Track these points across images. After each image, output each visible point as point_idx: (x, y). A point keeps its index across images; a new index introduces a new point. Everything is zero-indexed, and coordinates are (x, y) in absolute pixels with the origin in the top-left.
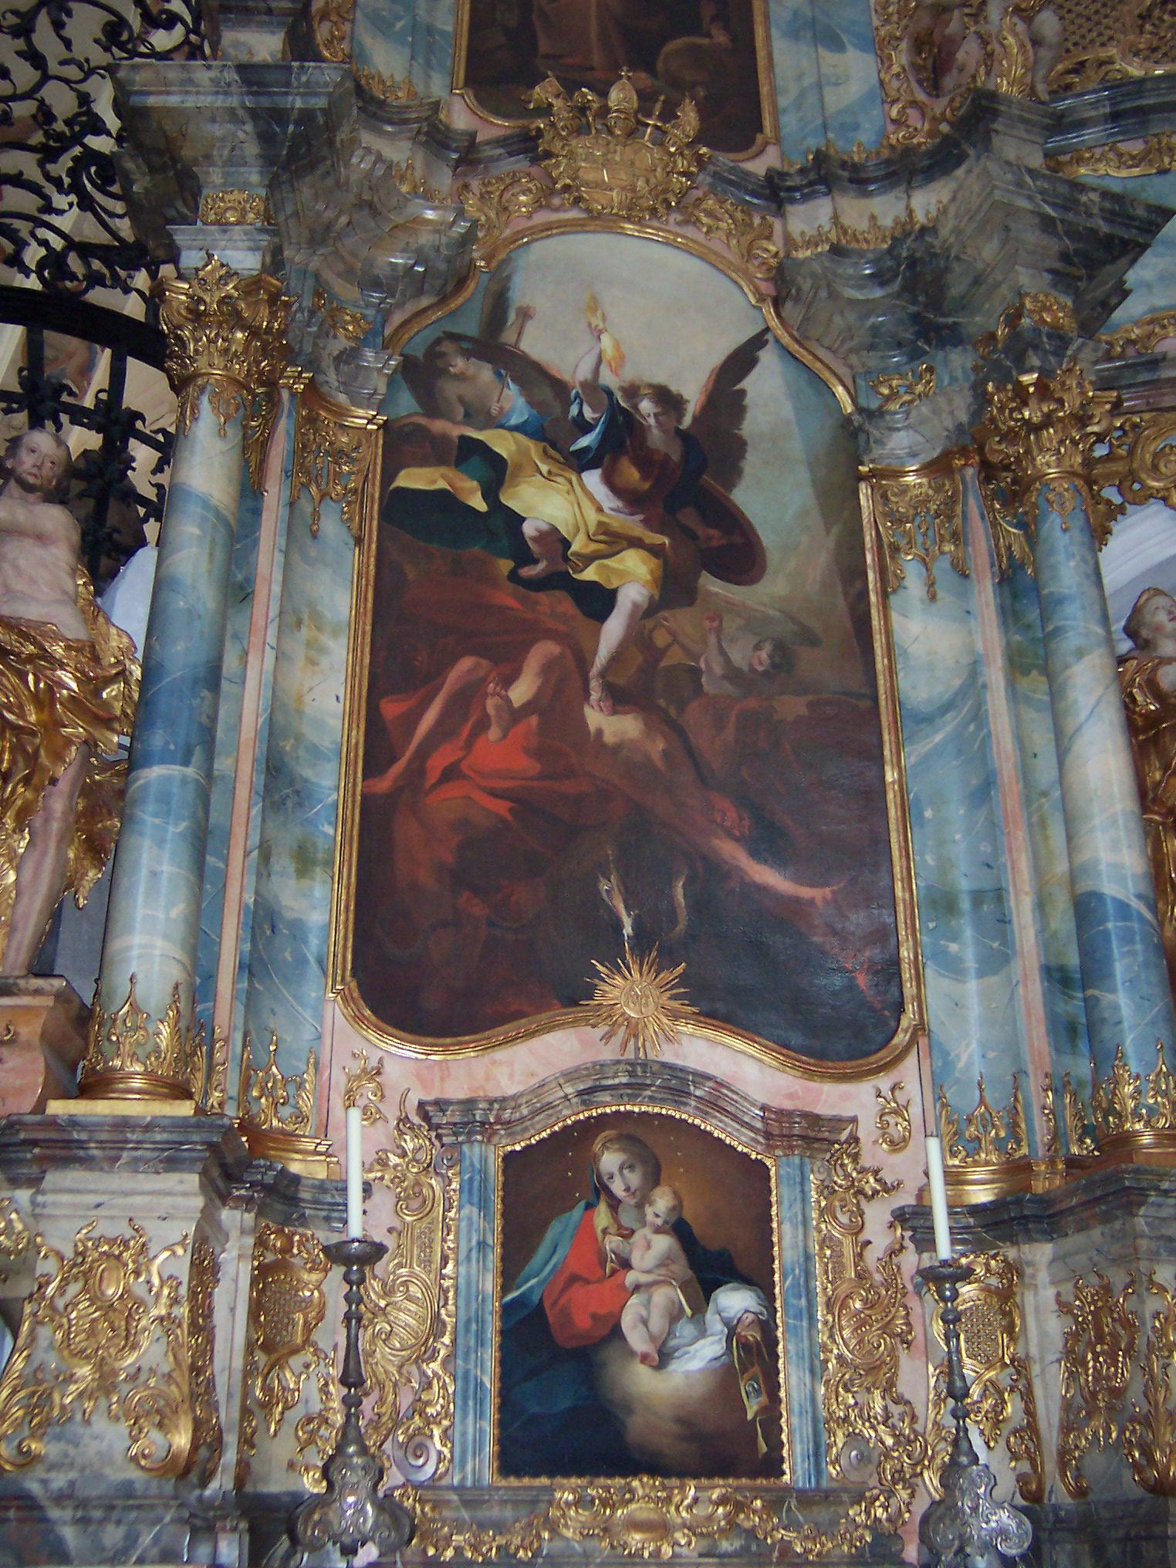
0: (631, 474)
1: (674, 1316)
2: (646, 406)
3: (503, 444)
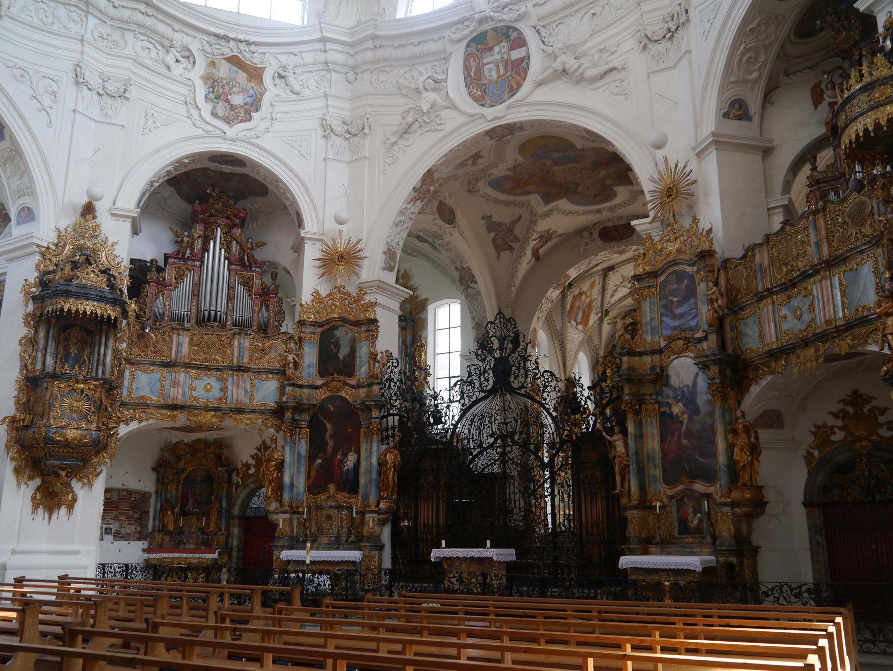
3: (670, 401)
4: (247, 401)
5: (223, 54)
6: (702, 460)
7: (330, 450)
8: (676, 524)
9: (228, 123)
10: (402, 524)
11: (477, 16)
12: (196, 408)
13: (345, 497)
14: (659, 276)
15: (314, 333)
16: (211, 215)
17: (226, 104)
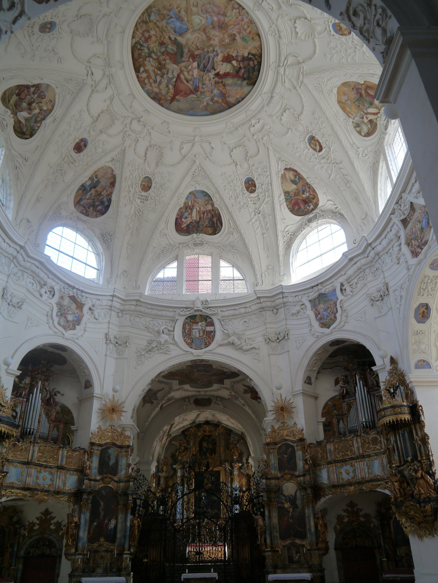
3: (283, 501)
4: (62, 487)
5: (69, 294)
7: (101, 517)
8: (287, 559)
9: (65, 329)
10: (144, 561)
11: (195, 308)
12: (36, 490)
13: (108, 545)
15: (98, 450)
16: (38, 374)
17: (65, 319)
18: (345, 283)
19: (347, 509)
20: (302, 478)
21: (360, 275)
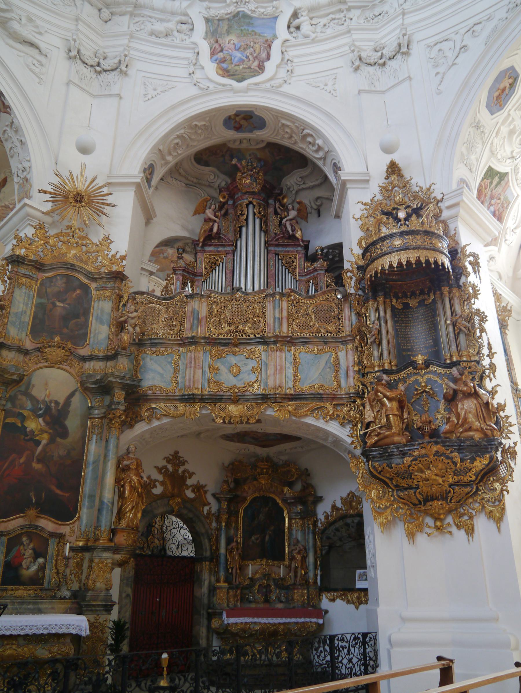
0: (48, 418)
1: (31, 562)
2: (53, 405)
3: (25, 413)
6: (58, 492)
14: (44, 271)
18: (304, 14)
19: (165, 467)
20: (99, 365)
21: (337, 16)
